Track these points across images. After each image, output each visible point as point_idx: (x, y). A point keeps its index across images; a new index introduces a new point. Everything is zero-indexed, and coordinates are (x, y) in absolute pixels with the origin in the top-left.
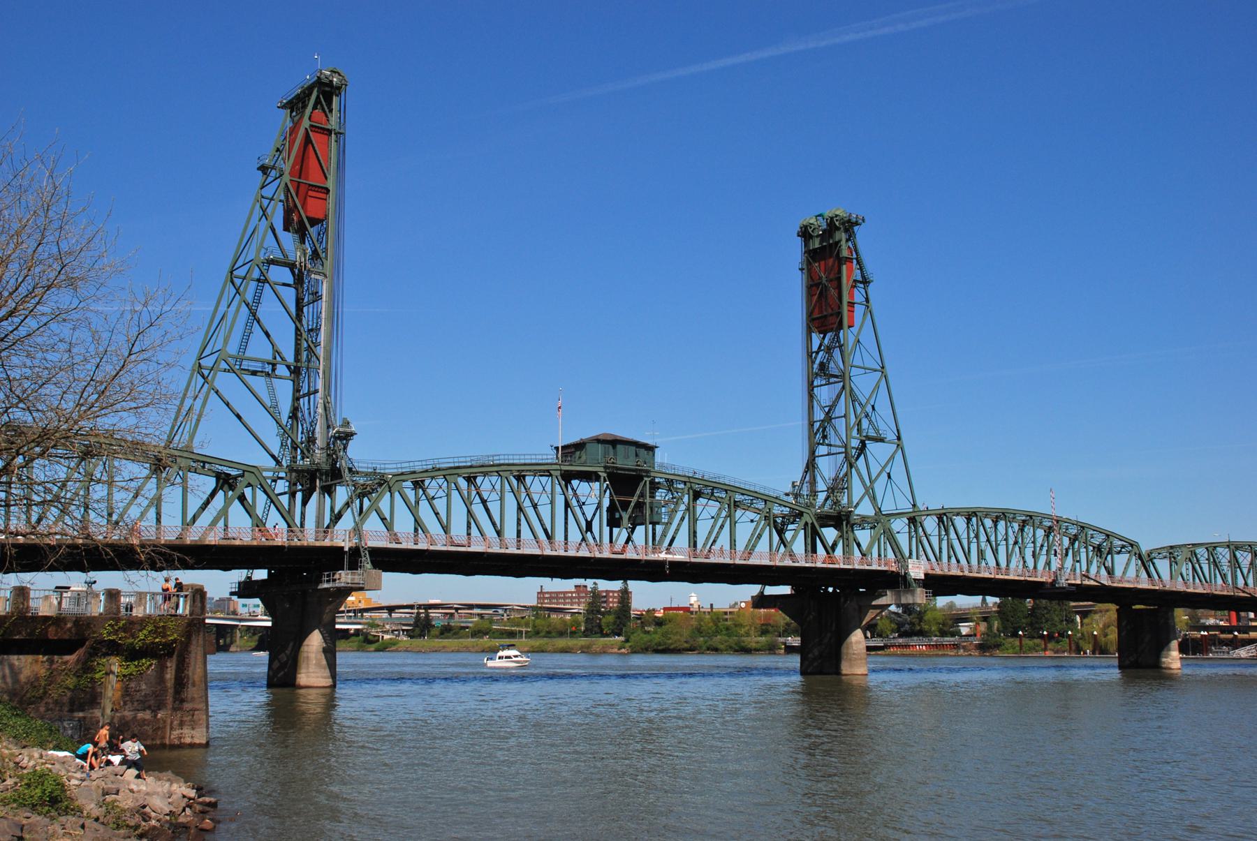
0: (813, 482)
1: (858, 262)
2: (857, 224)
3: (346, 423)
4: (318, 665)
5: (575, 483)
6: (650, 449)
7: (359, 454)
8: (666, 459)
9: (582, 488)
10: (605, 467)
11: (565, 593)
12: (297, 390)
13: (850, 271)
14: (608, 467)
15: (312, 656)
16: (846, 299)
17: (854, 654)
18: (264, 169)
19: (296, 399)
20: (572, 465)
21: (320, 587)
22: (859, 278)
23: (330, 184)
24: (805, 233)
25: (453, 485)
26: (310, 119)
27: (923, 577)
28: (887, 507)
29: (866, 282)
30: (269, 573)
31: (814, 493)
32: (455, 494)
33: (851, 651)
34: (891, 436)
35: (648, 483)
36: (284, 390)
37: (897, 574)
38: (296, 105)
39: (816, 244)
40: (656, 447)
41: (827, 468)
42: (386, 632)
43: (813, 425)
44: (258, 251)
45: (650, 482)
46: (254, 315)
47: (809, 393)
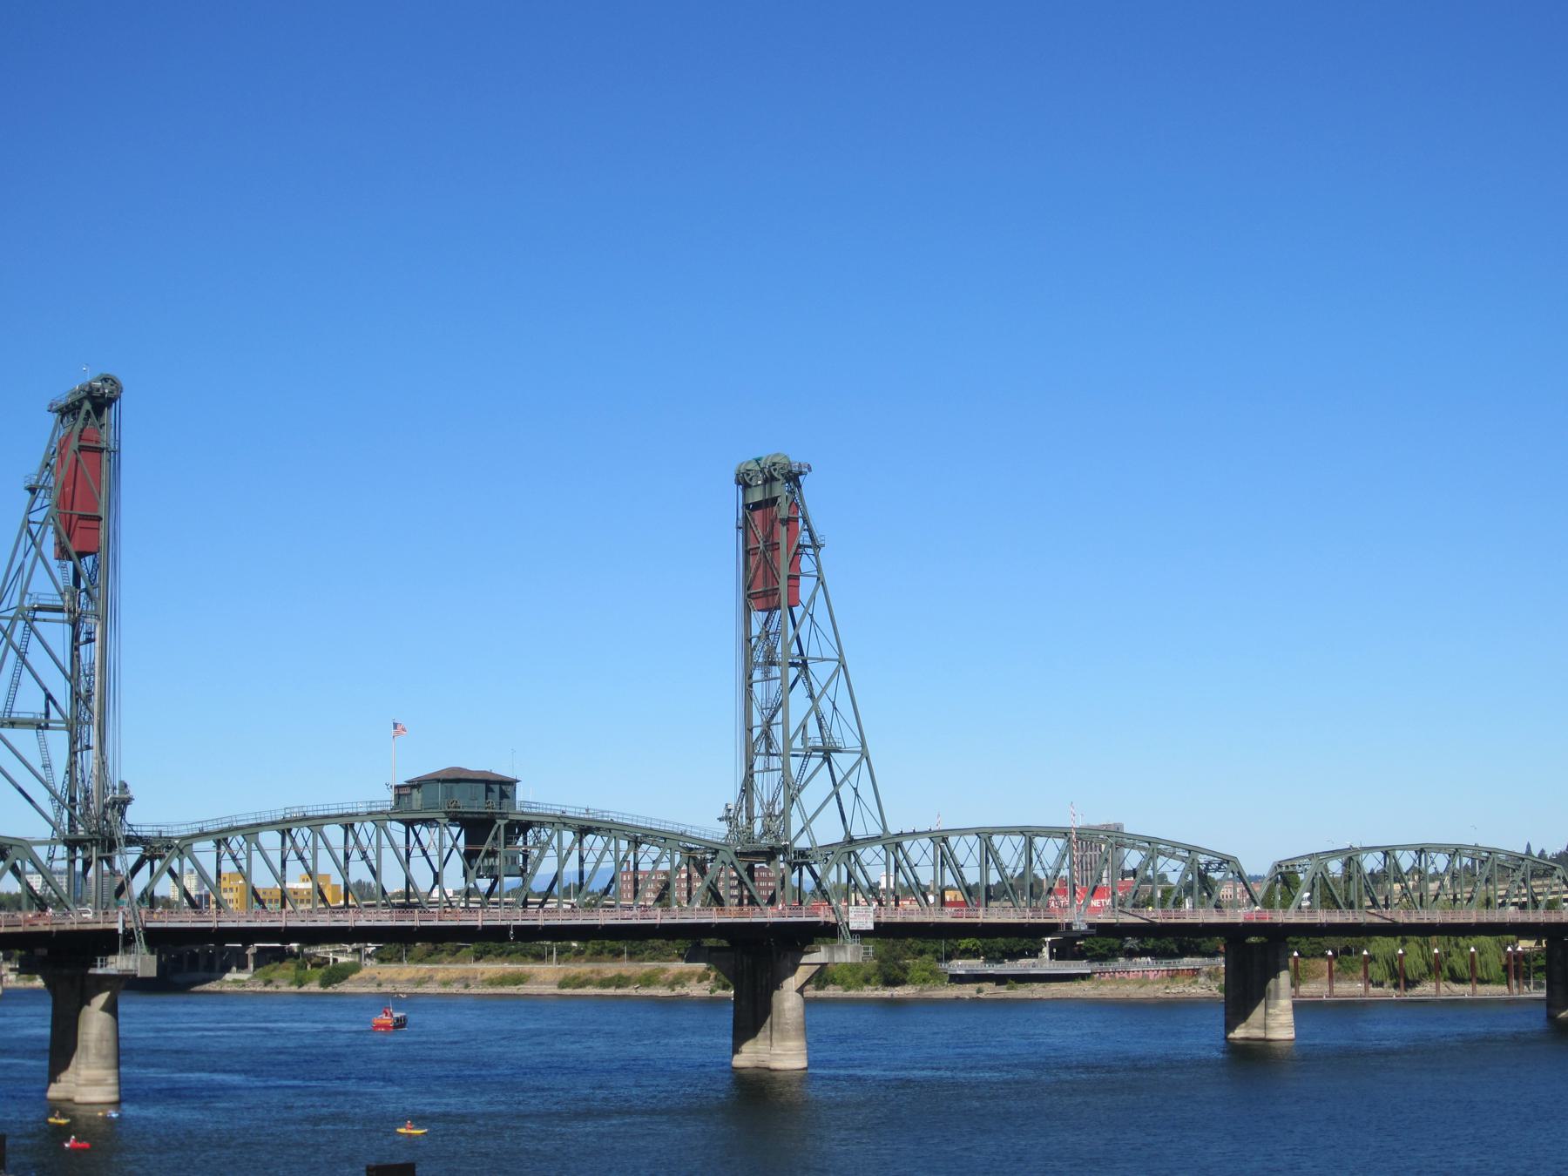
0: (750, 809)
1: (806, 521)
2: (801, 473)
3: (124, 786)
4: (99, 1055)
5: (417, 828)
6: (512, 783)
7: (141, 817)
8: (530, 796)
9: (424, 833)
10: (446, 813)
12: (73, 742)
13: (792, 534)
14: (450, 812)
15: (92, 1045)
16: (784, 571)
17: (787, 1024)
18: (32, 490)
19: (73, 753)
20: (402, 813)
21: (91, 971)
22: (808, 541)
23: (102, 513)
24: (744, 482)
25: (253, 845)
26: (80, 438)
27: (871, 927)
28: (858, 832)
29: (816, 546)
31: (750, 819)
32: (256, 855)
33: (783, 1021)
34: (852, 742)
35: (502, 827)
36: (58, 741)
37: (836, 925)
38: (68, 411)
39: (757, 496)
40: (519, 781)
41: (767, 784)
43: (751, 730)
44: (22, 599)
45: (505, 825)
46: (24, 661)
47: (746, 690)
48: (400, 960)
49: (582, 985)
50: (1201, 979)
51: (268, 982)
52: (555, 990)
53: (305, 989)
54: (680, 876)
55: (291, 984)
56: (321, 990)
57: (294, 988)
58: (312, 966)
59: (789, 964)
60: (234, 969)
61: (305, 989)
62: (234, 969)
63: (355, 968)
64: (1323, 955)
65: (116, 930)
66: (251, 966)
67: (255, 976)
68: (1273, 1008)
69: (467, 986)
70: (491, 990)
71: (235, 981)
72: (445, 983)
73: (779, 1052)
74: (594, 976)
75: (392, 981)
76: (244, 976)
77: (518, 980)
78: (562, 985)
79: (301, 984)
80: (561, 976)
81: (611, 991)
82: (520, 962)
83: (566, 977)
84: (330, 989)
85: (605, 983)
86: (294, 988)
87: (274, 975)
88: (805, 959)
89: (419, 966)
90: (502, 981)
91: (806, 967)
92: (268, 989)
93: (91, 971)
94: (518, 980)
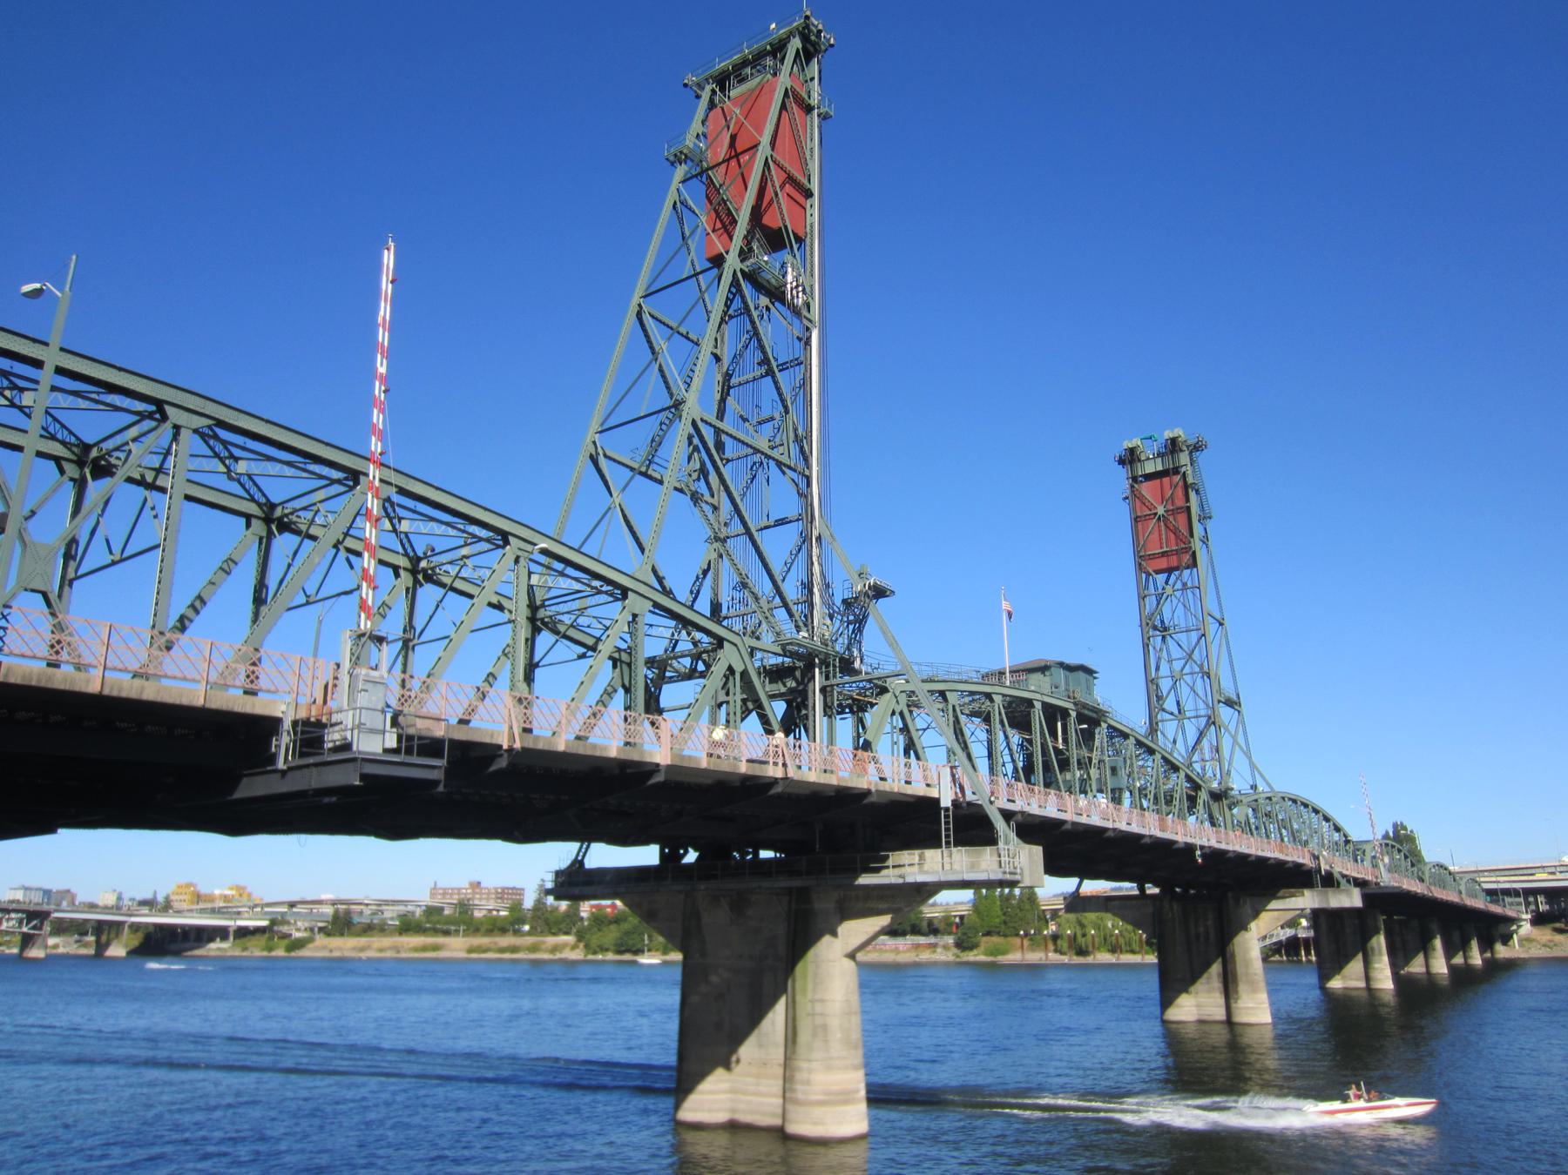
11: (459, 889)
15: (834, 1023)
30: (662, 855)
42: (298, 930)
48: (342, 934)
49: (485, 951)
50: (939, 950)
51: (245, 949)
52: (464, 955)
53: (274, 954)
54: (756, 854)
55: (263, 950)
56: (286, 954)
57: (265, 954)
58: (279, 938)
59: (1250, 911)
60: (218, 939)
61: (274, 954)
62: (218, 939)
63: (310, 940)
64: (1017, 935)
65: (937, 801)
66: (231, 938)
67: (234, 945)
68: (1379, 963)
69: (398, 952)
70: (416, 955)
71: (219, 949)
72: (381, 950)
73: (1251, 1005)
74: (492, 946)
75: (340, 949)
76: (225, 945)
77: (436, 948)
78: (470, 951)
79: (270, 949)
80: (467, 946)
81: (507, 956)
82: (433, 936)
83: (471, 946)
84: (293, 954)
85: (502, 950)
86: (265, 954)
87: (248, 944)
88: (1274, 905)
89: (358, 939)
90: (424, 949)
91: (1276, 913)
92: (245, 954)
93: (865, 880)
94: (436, 948)
